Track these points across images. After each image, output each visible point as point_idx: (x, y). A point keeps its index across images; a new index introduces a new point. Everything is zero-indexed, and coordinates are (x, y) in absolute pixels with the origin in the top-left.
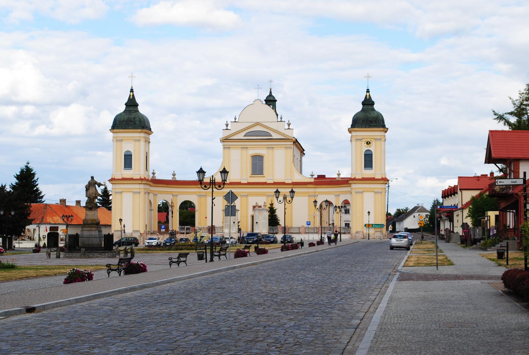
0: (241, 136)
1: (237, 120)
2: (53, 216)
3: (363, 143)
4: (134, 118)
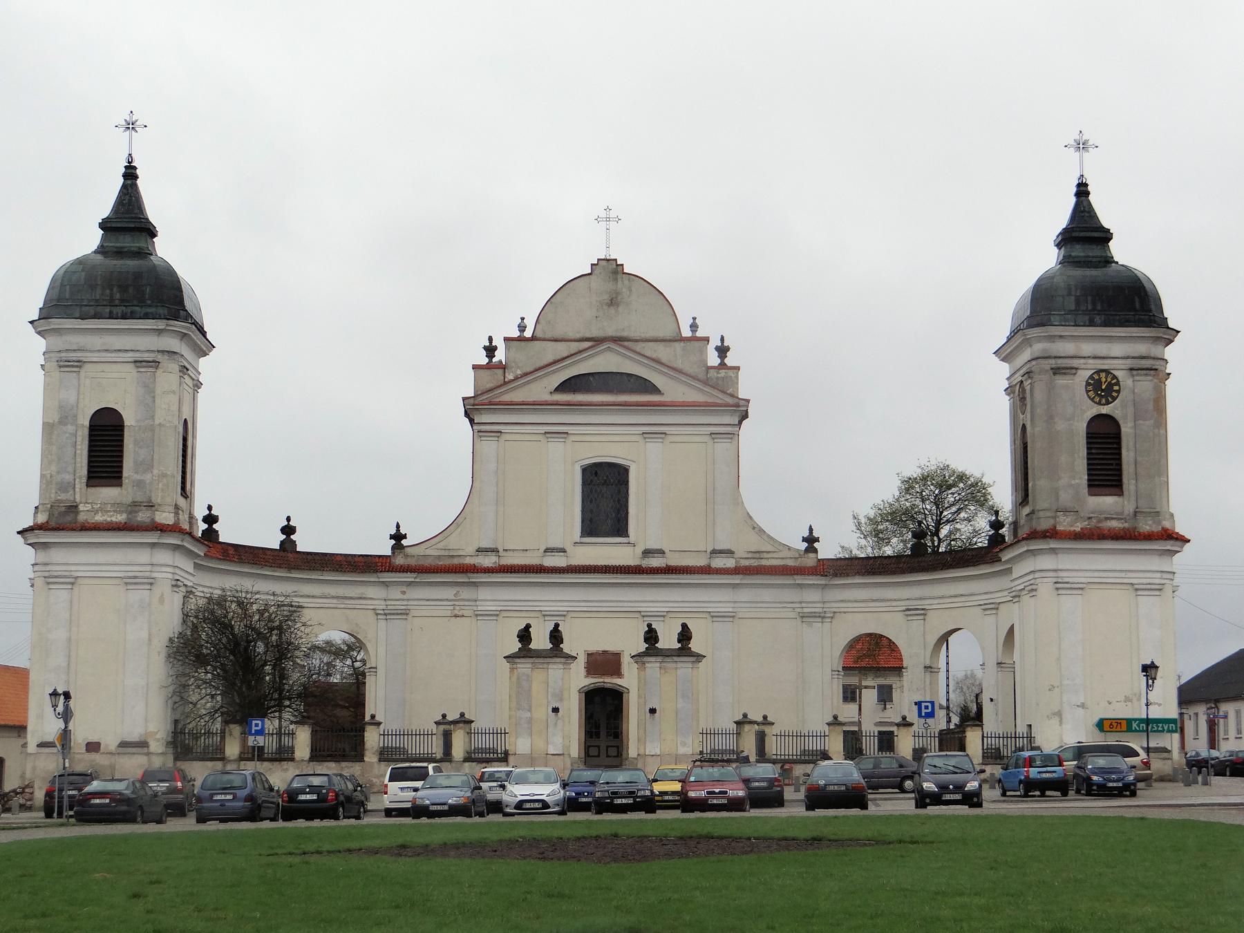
1: (528, 334)
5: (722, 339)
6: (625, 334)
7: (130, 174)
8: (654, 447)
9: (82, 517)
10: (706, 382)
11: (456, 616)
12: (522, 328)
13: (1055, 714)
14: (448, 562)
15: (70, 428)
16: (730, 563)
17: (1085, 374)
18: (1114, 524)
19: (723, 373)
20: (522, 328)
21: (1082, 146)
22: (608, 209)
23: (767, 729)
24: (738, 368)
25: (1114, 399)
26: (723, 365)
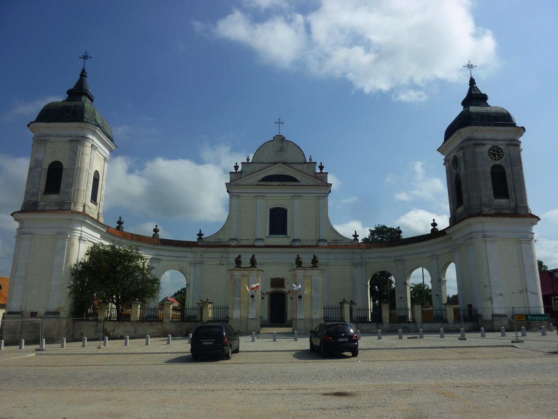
1: (250, 161)
5: (321, 164)
6: (286, 161)
7: (83, 74)
8: (297, 202)
9: (40, 208)
10: (316, 178)
11: (221, 264)
12: (248, 160)
13: (489, 299)
14: (218, 244)
15: (39, 169)
16: (326, 244)
17: (488, 147)
18: (507, 211)
19: (322, 175)
20: (248, 160)
21: (470, 66)
22: (279, 119)
23: (353, 307)
24: (327, 173)
25: (501, 158)
26: (321, 172)
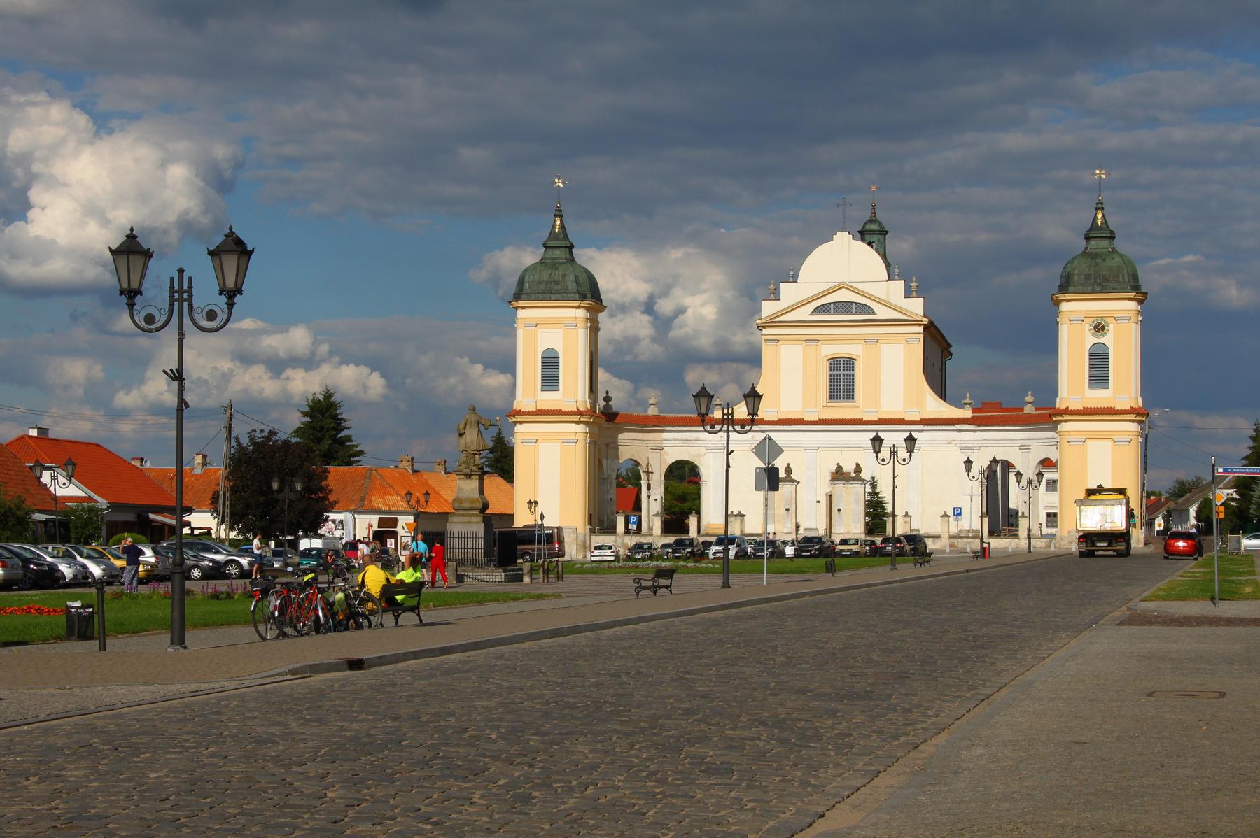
0: (804, 314)
2: (385, 494)
3: (1087, 327)
4: (564, 276)
17: (1088, 320)
